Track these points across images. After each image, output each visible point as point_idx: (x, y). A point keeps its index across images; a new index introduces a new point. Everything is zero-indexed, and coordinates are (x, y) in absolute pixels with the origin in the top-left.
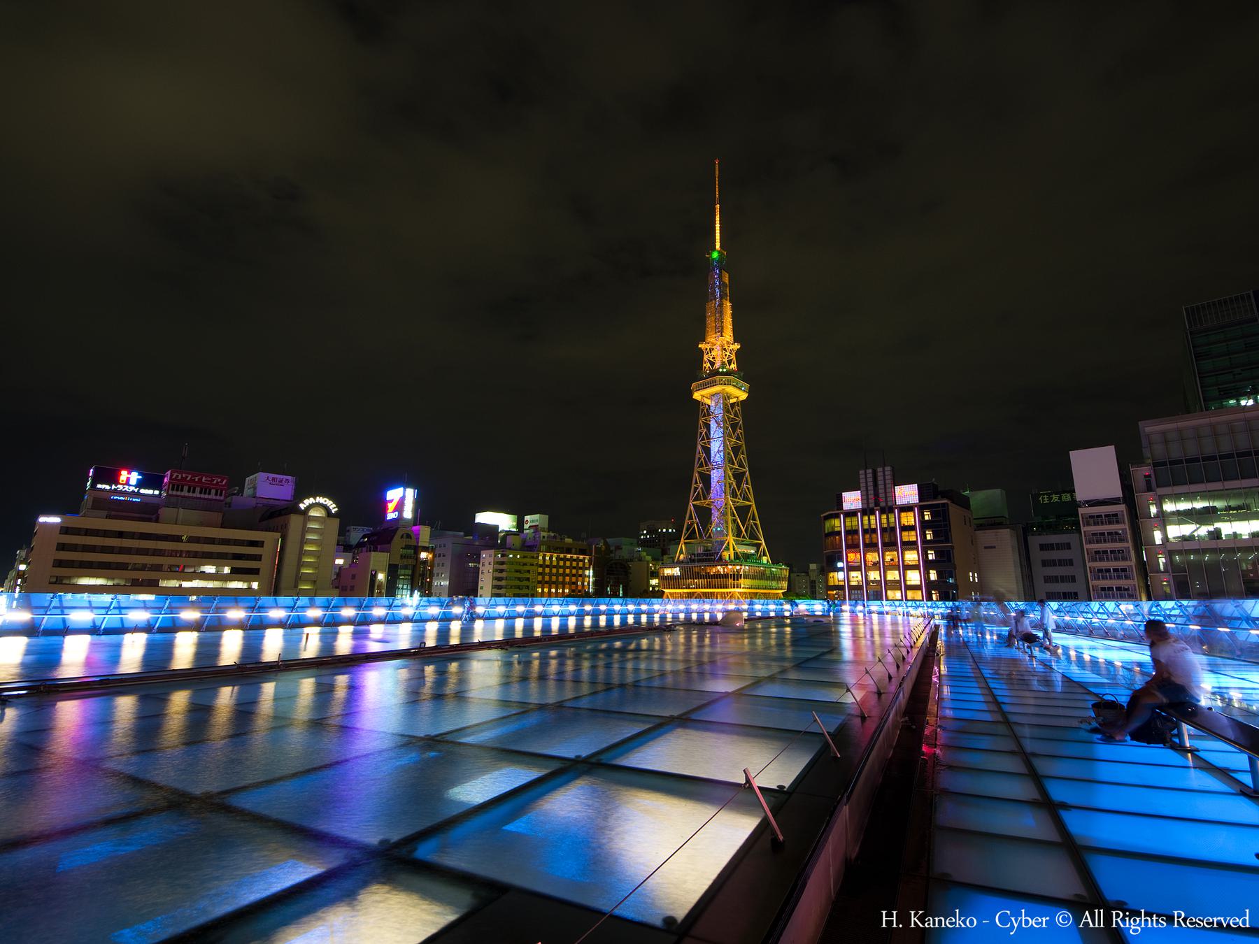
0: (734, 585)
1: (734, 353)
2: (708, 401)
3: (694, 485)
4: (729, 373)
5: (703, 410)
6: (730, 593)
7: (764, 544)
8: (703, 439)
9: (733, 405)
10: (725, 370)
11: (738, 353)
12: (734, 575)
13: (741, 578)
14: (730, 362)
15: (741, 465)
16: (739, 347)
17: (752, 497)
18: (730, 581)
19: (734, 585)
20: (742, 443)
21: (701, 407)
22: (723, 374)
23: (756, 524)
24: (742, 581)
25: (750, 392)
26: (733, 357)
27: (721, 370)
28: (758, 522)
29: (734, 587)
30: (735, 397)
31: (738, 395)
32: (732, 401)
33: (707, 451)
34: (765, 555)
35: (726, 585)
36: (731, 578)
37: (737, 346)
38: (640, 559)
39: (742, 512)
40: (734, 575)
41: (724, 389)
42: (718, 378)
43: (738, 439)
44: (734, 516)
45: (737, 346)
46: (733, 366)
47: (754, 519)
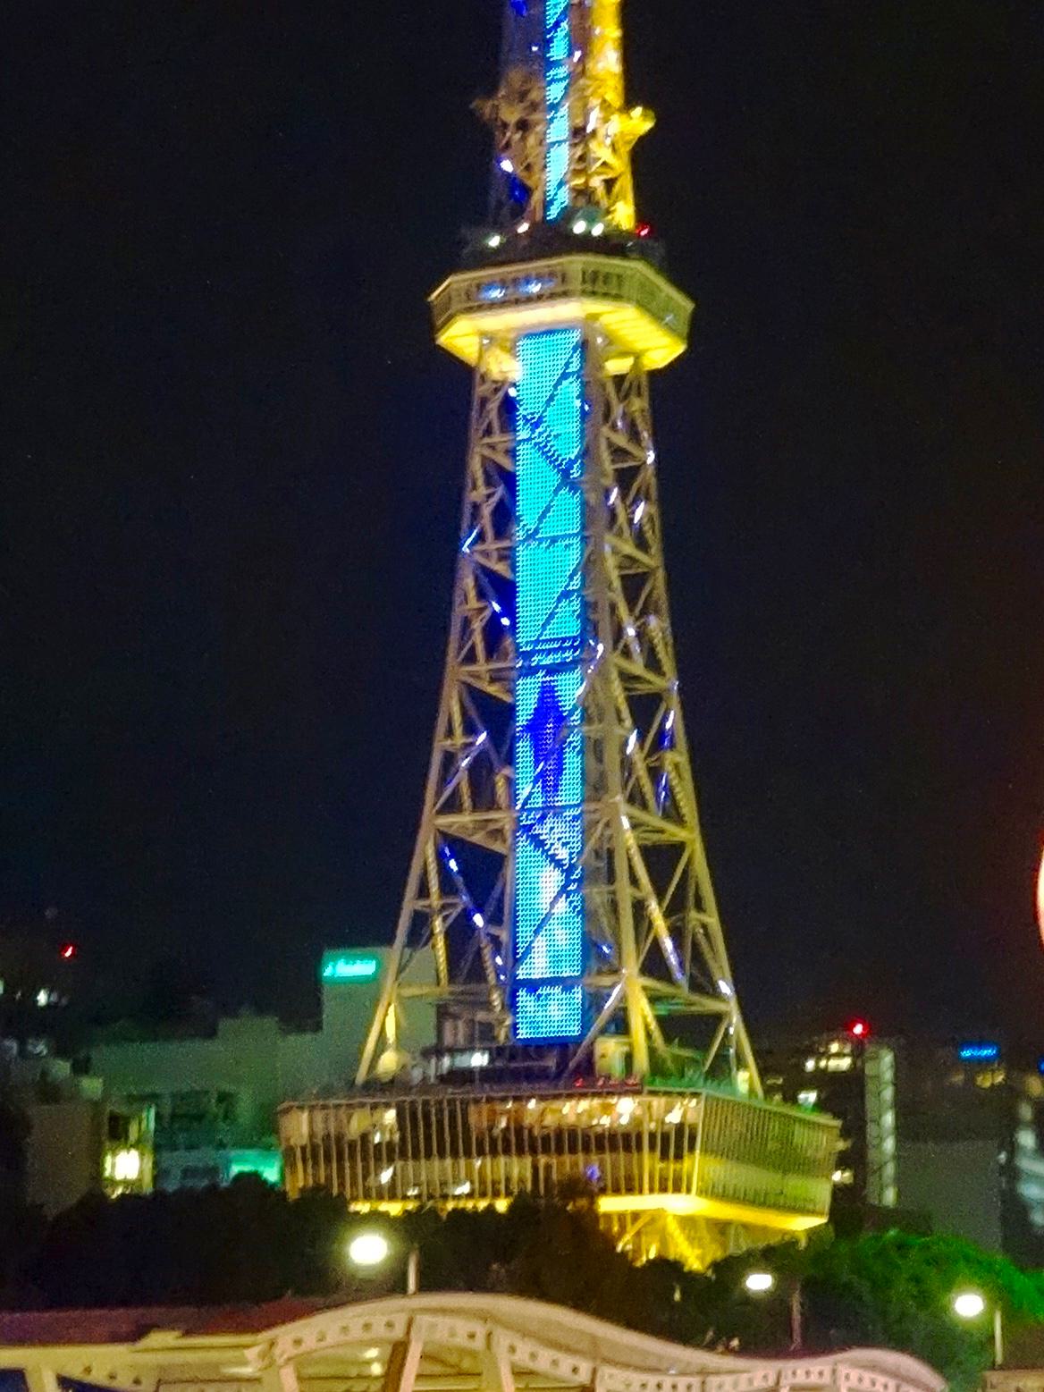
0: (664, 1181)
1: (625, 150)
2: (501, 366)
3: (441, 744)
4: (612, 245)
5: (484, 402)
6: (636, 1216)
7: (735, 1024)
8: (481, 538)
9: (619, 380)
10: (597, 230)
11: (643, 154)
12: (665, 1137)
13: (692, 1148)
14: (609, 184)
15: (653, 663)
16: (647, 125)
17: (688, 806)
18: (649, 1162)
19: (664, 1181)
20: (652, 560)
21: (480, 390)
22: (586, 244)
23: (704, 926)
24: (696, 1165)
25: (697, 333)
26: (620, 165)
27: (579, 227)
28: (713, 920)
29: (664, 1189)
30: (624, 354)
31: (639, 346)
32: (617, 366)
33: (505, 591)
34: (741, 1063)
35: (629, 1179)
36: (652, 1147)
37: (639, 122)
38: (50, 1092)
39: (661, 859)
40: (665, 1137)
41: (594, 317)
42: (576, 263)
43: (642, 544)
44: (634, 881)
45: (639, 122)
46: (624, 214)
47: (699, 906)
